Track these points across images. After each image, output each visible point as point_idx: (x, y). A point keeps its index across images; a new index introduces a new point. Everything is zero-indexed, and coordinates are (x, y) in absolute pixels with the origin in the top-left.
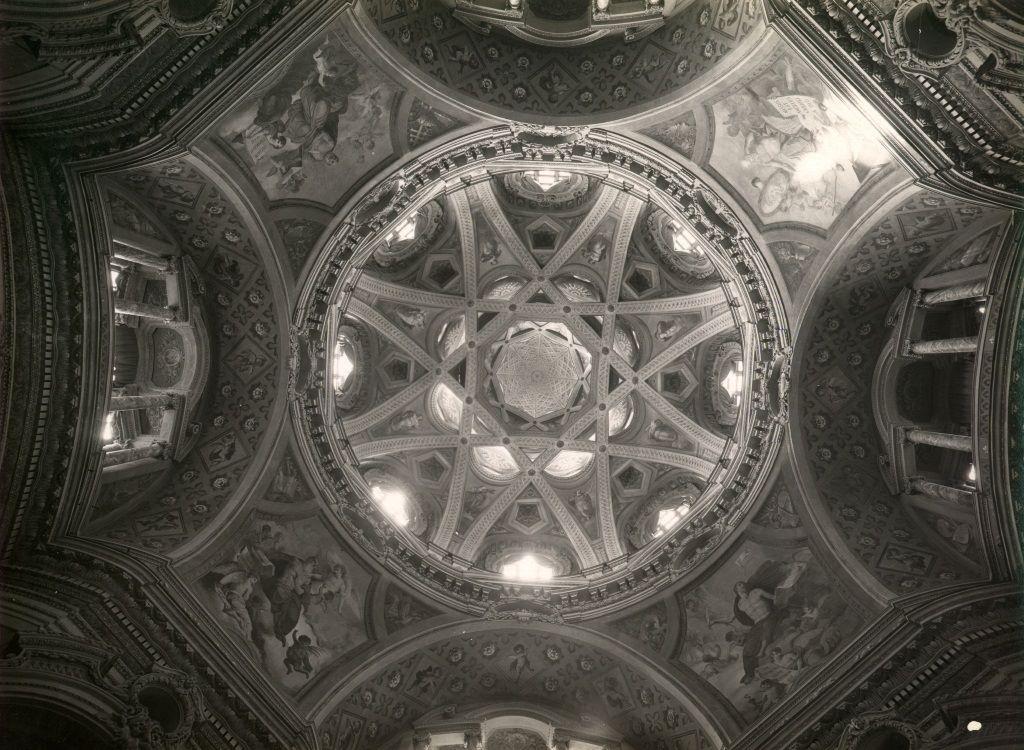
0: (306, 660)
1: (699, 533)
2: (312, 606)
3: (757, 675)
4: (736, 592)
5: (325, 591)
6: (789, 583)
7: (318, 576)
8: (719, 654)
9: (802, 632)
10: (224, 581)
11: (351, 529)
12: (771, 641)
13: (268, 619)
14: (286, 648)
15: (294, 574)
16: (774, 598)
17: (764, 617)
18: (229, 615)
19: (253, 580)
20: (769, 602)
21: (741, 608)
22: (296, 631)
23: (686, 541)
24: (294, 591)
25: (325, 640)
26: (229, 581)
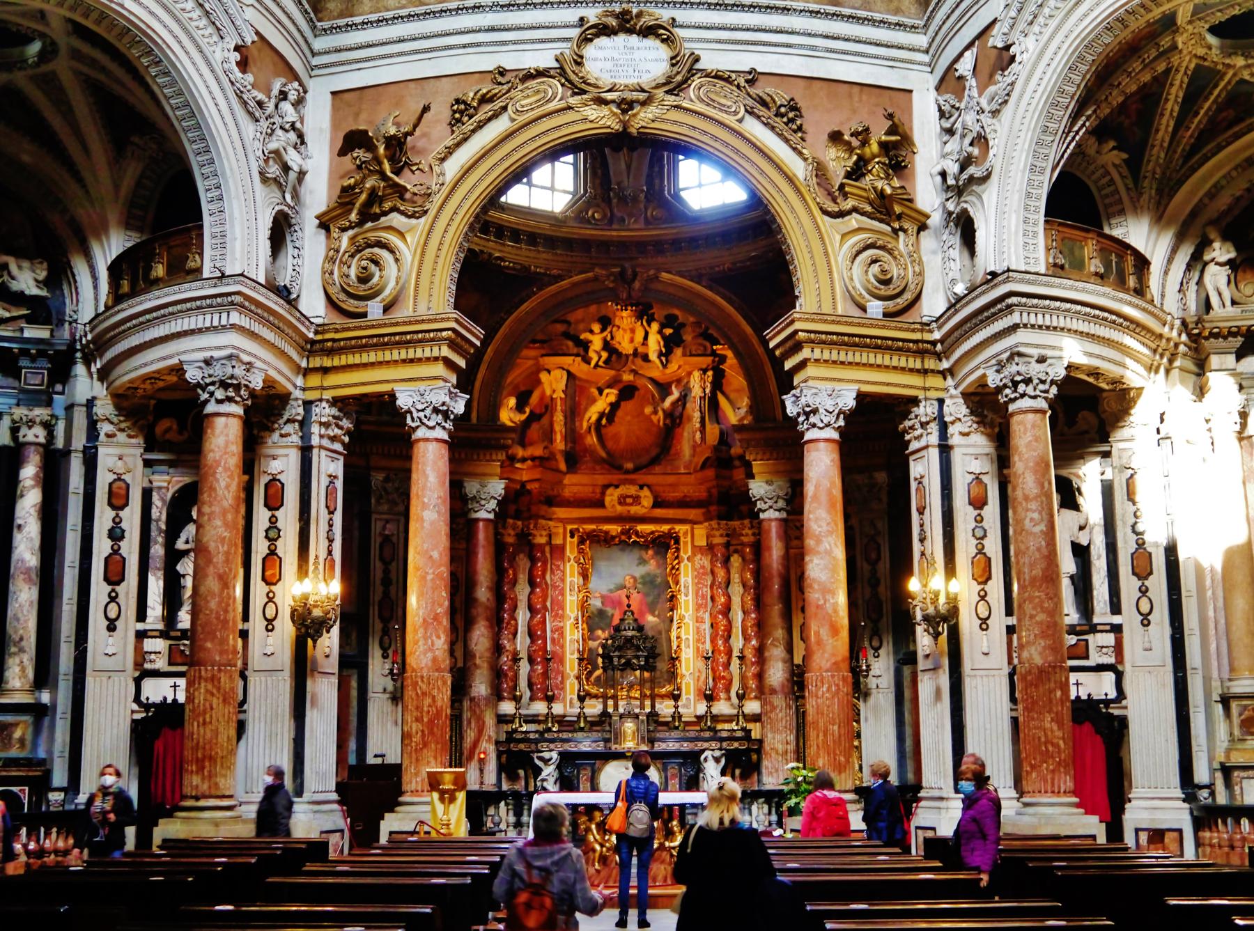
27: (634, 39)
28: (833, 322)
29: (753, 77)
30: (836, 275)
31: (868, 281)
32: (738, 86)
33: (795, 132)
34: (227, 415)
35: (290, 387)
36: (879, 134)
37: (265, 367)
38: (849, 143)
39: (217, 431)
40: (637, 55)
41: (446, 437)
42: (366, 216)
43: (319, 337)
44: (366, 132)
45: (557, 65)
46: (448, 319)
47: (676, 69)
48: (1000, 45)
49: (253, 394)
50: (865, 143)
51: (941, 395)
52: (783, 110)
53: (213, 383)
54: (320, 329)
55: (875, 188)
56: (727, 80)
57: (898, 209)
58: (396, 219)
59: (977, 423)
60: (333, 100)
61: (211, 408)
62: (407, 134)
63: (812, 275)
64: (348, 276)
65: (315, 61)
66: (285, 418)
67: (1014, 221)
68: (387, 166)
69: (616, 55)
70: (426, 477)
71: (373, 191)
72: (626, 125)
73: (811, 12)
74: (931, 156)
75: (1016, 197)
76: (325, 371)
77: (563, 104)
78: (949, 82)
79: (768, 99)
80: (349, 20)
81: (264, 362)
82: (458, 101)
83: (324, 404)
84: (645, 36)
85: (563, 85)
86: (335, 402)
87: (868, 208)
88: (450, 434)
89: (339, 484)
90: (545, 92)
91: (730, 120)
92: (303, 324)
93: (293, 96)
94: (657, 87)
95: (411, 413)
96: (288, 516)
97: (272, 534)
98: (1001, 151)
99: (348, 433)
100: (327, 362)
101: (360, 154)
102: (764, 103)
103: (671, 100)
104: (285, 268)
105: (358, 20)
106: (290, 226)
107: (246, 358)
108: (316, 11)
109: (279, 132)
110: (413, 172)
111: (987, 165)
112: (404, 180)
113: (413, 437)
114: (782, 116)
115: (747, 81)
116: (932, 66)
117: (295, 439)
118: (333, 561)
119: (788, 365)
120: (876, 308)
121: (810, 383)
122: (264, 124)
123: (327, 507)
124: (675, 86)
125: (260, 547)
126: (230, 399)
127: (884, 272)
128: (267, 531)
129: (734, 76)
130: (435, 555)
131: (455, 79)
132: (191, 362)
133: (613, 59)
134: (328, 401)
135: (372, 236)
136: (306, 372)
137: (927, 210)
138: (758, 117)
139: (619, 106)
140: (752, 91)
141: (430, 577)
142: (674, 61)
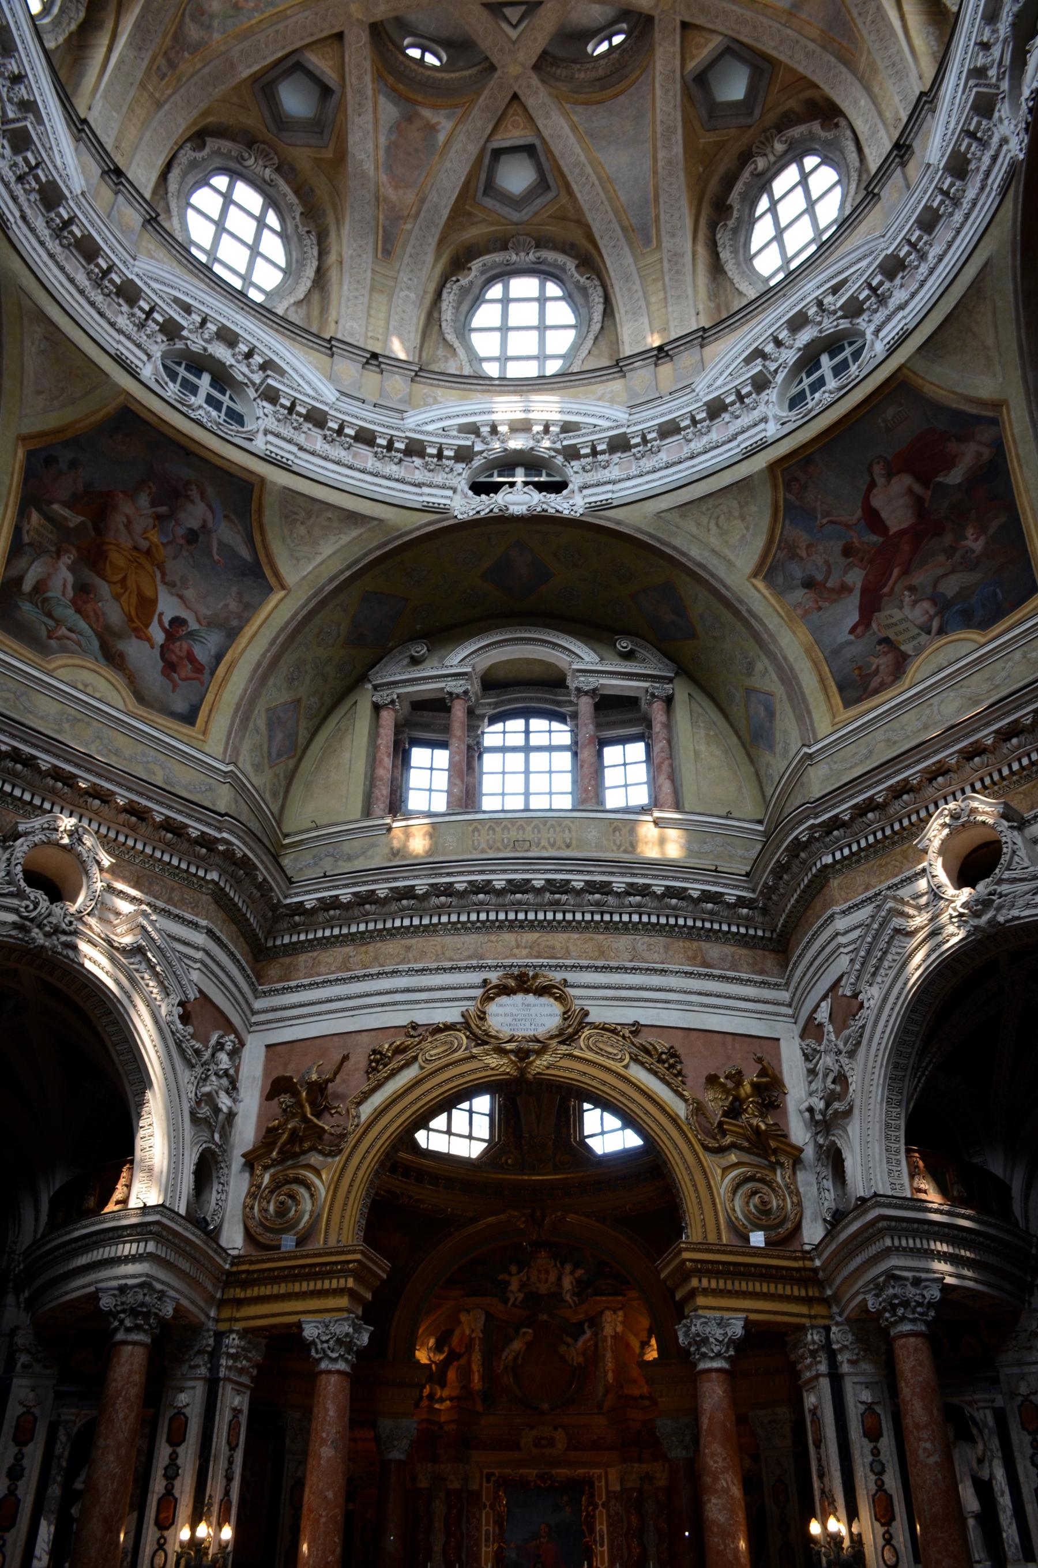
0: (191, 658)
1: (829, 325)
2: (169, 565)
3: (874, 625)
4: (871, 475)
5: (180, 531)
6: (955, 477)
7: (163, 510)
8: (826, 580)
9: (953, 571)
10: (27, 586)
11: (189, 406)
12: (906, 572)
13: (114, 614)
14: (157, 652)
15: (124, 520)
16: (927, 495)
17: (904, 525)
18: (58, 638)
19: (66, 560)
20: (919, 500)
21: (876, 502)
22: (161, 614)
23: (805, 336)
24: (136, 548)
25: (209, 613)
26: (34, 581)
27: (531, 998)
28: (718, 1252)
29: (637, 1028)
30: (719, 1206)
31: (750, 1211)
32: (624, 1037)
33: (676, 1076)
34: (135, 1343)
35: (202, 1317)
36: (751, 1075)
37: (177, 1296)
38: (723, 1085)
39: (123, 1360)
40: (533, 1011)
41: (348, 1370)
42: (286, 1154)
43: (235, 1269)
44: (291, 1078)
45: (462, 1020)
46: (354, 1252)
47: (567, 1023)
48: (849, 994)
49: (162, 1322)
50: (739, 1084)
51: (826, 1322)
52: (664, 1057)
53: (123, 1311)
54: (237, 1260)
55: (751, 1125)
56: (614, 1031)
57: (773, 1144)
58: (315, 1159)
59: (865, 1350)
60: (267, 1052)
61: (120, 1336)
62: (328, 1081)
63: (696, 1207)
64: (266, 1210)
65: (254, 1019)
66: (196, 1348)
67: (877, 1149)
68: (308, 1109)
69: (514, 1011)
70: (327, 1410)
71: (294, 1132)
72: (522, 1071)
74: (798, 1093)
75: (877, 1127)
76: (239, 1303)
77: (467, 1054)
78: (811, 1030)
79: (650, 1048)
80: (286, 984)
81: (177, 1291)
82: (374, 1052)
83: (234, 1336)
84: (541, 995)
85: (467, 1037)
86: (244, 1334)
87: (746, 1144)
88: (353, 1366)
89: (243, 1419)
90: (452, 1043)
91: (617, 1066)
92: (219, 1255)
93: (229, 1046)
94: (551, 1038)
95: (316, 1344)
96: (188, 1456)
97: (170, 1472)
99: (258, 1366)
100: (240, 1294)
101: (286, 1099)
102: (647, 1051)
104: (209, 1202)
105: (293, 984)
106: (217, 1162)
107: (159, 1286)
108: (259, 977)
109: (214, 1078)
110: (332, 1115)
111: (848, 1099)
112: (325, 1124)
113: (317, 1369)
114: (663, 1062)
115: (631, 1032)
116: (795, 1017)
117: (203, 1371)
118: (230, 1502)
119: (679, 1296)
120: (757, 1239)
121: (700, 1312)
122: (199, 1070)
123: (229, 1443)
124: (567, 1036)
125: (158, 1486)
126: (138, 1328)
127: (764, 1203)
128: (166, 1469)
129: (619, 1028)
130: (330, 1495)
131: (374, 1033)
132: (105, 1290)
134: (237, 1332)
135: (291, 1173)
136: (221, 1304)
137: (800, 1144)
138: (642, 1064)
139: (516, 1056)
140: (635, 1040)
141: (323, 1520)
142: (566, 1016)
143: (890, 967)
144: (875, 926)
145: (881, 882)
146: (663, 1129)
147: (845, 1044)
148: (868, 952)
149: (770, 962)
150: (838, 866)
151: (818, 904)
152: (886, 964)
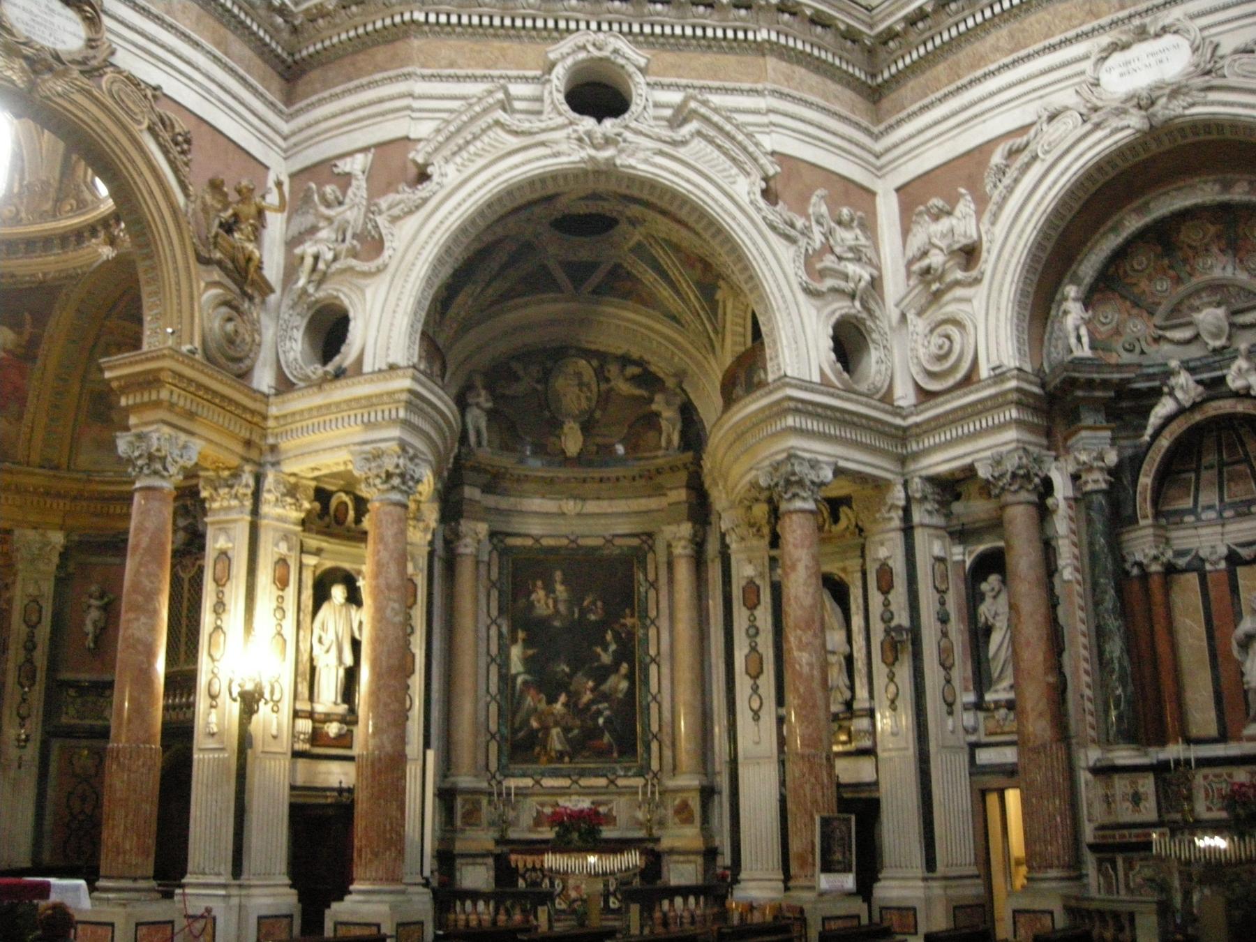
32: (145, 96)
38: (225, 195)
40: (57, 20)
52: (180, 139)
73: (215, 57)
79: (168, 122)
87: (230, 265)
91: (135, 128)
94: (74, 62)
98: (399, 254)
103: (84, 82)
114: (177, 144)
129: (143, 86)
133: (31, 12)
138: (155, 136)
142: (91, 43)
143: (476, 154)
144: (477, 109)
145: (469, 66)
146: (162, 217)
147: (390, 208)
148: (459, 130)
149: (277, 82)
150: (426, 28)
151: (381, 54)
152: (472, 149)
